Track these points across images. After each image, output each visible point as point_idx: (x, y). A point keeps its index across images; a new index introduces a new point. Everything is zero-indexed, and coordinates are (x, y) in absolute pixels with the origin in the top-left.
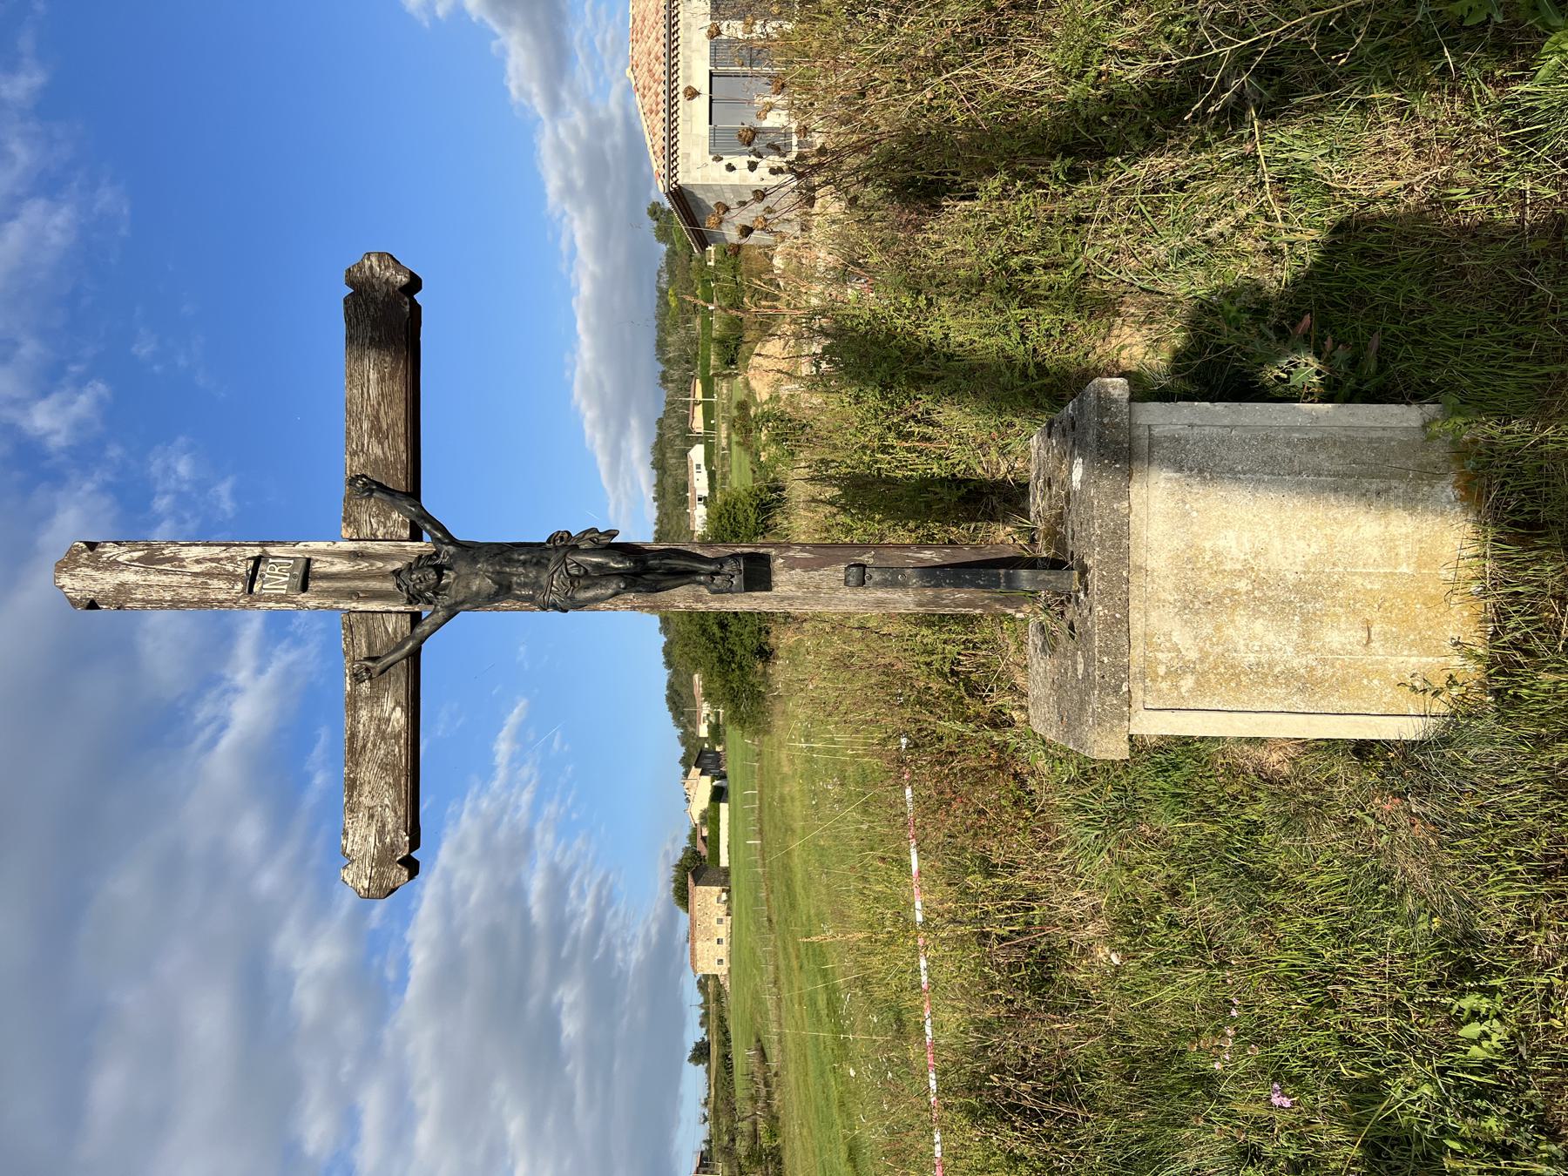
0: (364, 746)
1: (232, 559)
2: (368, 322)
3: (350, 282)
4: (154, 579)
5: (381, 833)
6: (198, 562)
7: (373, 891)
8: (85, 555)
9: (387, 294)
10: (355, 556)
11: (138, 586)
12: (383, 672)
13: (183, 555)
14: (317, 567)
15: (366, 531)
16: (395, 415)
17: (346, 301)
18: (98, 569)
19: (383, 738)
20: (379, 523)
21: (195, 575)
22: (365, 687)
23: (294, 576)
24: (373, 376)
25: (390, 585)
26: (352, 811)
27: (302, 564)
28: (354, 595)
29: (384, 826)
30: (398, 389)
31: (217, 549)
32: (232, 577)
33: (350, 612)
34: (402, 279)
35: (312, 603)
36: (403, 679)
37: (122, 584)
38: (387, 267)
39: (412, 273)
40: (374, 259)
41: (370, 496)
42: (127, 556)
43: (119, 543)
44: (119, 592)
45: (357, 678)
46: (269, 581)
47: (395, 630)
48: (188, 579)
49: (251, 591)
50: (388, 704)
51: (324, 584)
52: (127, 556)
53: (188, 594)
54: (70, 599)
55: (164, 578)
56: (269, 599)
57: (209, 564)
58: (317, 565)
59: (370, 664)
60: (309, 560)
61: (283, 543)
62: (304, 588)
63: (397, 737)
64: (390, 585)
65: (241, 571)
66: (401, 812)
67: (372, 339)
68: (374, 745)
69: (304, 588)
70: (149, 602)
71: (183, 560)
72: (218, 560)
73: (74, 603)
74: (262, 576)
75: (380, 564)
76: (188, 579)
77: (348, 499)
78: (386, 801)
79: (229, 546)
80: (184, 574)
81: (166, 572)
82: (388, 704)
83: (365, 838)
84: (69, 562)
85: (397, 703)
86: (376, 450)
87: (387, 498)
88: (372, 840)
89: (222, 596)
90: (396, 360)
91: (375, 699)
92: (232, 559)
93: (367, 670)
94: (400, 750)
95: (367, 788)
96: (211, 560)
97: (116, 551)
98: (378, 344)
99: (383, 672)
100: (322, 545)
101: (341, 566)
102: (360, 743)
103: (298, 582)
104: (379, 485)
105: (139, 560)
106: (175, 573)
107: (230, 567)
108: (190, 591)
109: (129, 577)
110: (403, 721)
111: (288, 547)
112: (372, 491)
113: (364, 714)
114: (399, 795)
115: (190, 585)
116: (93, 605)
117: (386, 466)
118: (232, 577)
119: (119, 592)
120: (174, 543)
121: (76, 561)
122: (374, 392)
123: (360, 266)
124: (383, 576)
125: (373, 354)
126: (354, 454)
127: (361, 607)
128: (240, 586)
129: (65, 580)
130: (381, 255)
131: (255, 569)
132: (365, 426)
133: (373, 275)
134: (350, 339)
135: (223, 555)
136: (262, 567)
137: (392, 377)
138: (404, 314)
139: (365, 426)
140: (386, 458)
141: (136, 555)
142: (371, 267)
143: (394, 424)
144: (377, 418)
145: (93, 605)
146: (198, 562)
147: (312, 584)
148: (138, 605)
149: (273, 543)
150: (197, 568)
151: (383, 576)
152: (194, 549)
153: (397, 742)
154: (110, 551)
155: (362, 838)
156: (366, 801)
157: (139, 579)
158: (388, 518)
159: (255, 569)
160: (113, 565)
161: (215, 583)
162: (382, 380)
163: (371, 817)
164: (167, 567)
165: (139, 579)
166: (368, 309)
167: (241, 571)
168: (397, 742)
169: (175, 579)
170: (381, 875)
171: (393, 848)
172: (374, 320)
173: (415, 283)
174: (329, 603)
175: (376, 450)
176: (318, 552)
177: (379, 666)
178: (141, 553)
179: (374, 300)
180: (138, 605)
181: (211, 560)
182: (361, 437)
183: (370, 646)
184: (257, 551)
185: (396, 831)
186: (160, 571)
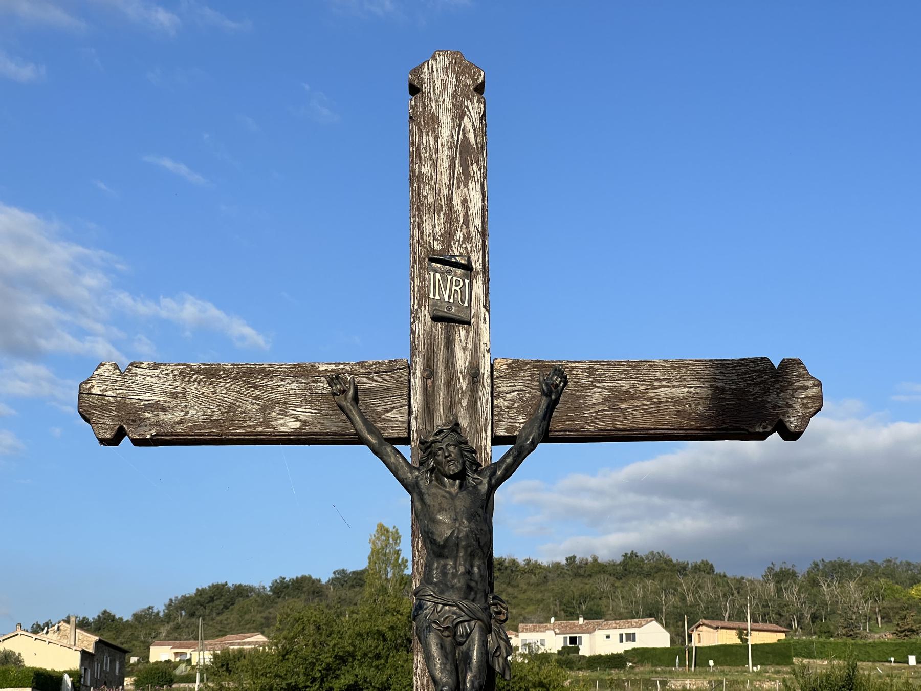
0: (255, 387)
1: (468, 238)
2: (741, 385)
3: (787, 365)
4: (444, 154)
5: (156, 407)
6: (464, 202)
7: (87, 398)
8: (470, 82)
9: (775, 407)
10: (474, 374)
11: (436, 138)
12: (341, 408)
13: (471, 185)
14: (461, 332)
15: (503, 386)
16: (635, 414)
17: (765, 360)
18: (455, 95)
19: (264, 408)
20: (513, 400)
21: (450, 198)
22: (323, 386)
23: (449, 308)
24: (680, 392)
25: (440, 420)
26: (181, 373)
27: (463, 316)
28: (429, 373)
29: (163, 409)
30: (667, 420)
31: (478, 222)
32: (447, 238)
33: (409, 368)
34: (793, 424)
35: (420, 328)
36: (333, 429)
37: (438, 122)
38: (805, 406)
39: (801, 433)
40: (814, 390)
41: (544, 393)
42: (469, 127)
43: (483, 117)
44: (430, 118)
45: (334, 379)
46: (444, 280)
47: (390, 420)
48: (445, 191)
49: (433, 260)
50: (304, 413)
51: (441, 339)
52: (469, 127)
53: (428, 191)
54: (421, 67)
55: (446, 165)
56: (423, 279)
57: (461, 213)
58: (463, 332)
59: (351, 393)
60: (469, 323)
61: (487, 293)
62: (436, 319)
63: (266, 423)
64: (440, 420)
65: (456, 250)
66: (179, 429)
67: (723, 390)
68: (256, 398)
69: (436, 319)
70: (419, 149)
71: (466, 185)
72: (466, 222)
73: (416, 71)
74: (449, 272)
75: (465, 403)
76: (445, 191)
77: (539, 364)
78: (192, 412)
79: (483, 234)
80: (450, 187)
81: (452, 168)
82: (304, 413)
83: (150, 389)
84: (461, 66)
85: (304, 423)
86: (596, 396)
87: (541, 412)
88: (148, 396)
89: (426, 227)
90: (700, 417)
91: (310, 399)
92: (468, 238)
93: (344, 391)
94: (251, 425)
95: (207, 390)
96: (466, 216)
97: (474, 115)
98: (717, 398)
99: (341, 408)
100: (485, 337)
101: (462, 359)
102: (259, 382)
103: (444, 311)
104: (556, 401)
105: (466, 139)
106: (451, 177)
107: (459, 236)
108: (432, 193)
109: (446, 128)
110: (284, 430)
111: (483, 299)
112: (548, 394)
113: (292, 386)
114: (199, 427)
115: (437, 193)
116: (414, 90)
117: (578, 408)
118: (447, 238)
119: (430, 118)
120: (485, 176)
121: (463, 73)
122: (663, 393)
123: (806, 375)
124: (451, 407)
125: (705, 391)
126: (591, 371)
127: (415, 382)
128: (437, 246)
129: (441, 62)
130: (819, 399)
131: (457, 265)
132: (623, 384)
133: (795, 390)
134: (722, 365)
135: (472, 228)
136: (460, 272)
137: (679, 413)
138: (753, 427)
139: (623, 384)
140: (587, 408)
141: (471, 136)
142: (805, 388)
143: (626, 416)
144: (633, 397)
145: (414, 90)
146: (464, 202)
147: (440, 326)
148: (415, 137)
149: (486, 282)
150: (457, 200)
151: (451, 407)
152: (479, 196)
153: (259, 424)
154: (474, 109)
155: (150, 387)
156: (193, 389)
157: (444, 138)
158: (518, 411)
159: (457, 265)
160: (459, 112)
161: (440, 221)
162: (676, 402)
163: (174, 395)
164: (458, 169)
165: (444, 138)
166: (756, 385)
167: (456, 250)
168: (259, 424)
169: (444, 177)
170: (106, 408)
171: (138, 421)
172: (744, 392)
173: (791, 436)
174: (420, 345)
175: (596, 396)
176: (477, 333)
177: (348, 404)
178: (473, 141)
179: (766, 392)
180: (415, 137)
181: (466, 216)
182: (611, 379)
183: (370, 392)
184: (477, 265)
185: (157, 424)
186: (453, 161)
